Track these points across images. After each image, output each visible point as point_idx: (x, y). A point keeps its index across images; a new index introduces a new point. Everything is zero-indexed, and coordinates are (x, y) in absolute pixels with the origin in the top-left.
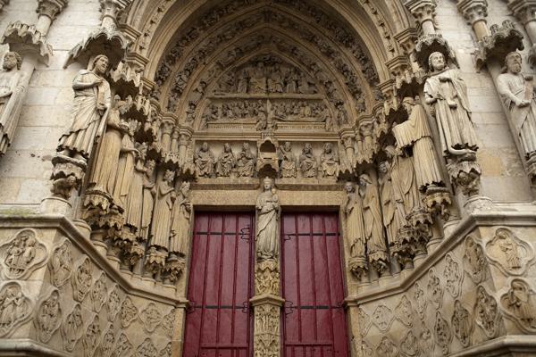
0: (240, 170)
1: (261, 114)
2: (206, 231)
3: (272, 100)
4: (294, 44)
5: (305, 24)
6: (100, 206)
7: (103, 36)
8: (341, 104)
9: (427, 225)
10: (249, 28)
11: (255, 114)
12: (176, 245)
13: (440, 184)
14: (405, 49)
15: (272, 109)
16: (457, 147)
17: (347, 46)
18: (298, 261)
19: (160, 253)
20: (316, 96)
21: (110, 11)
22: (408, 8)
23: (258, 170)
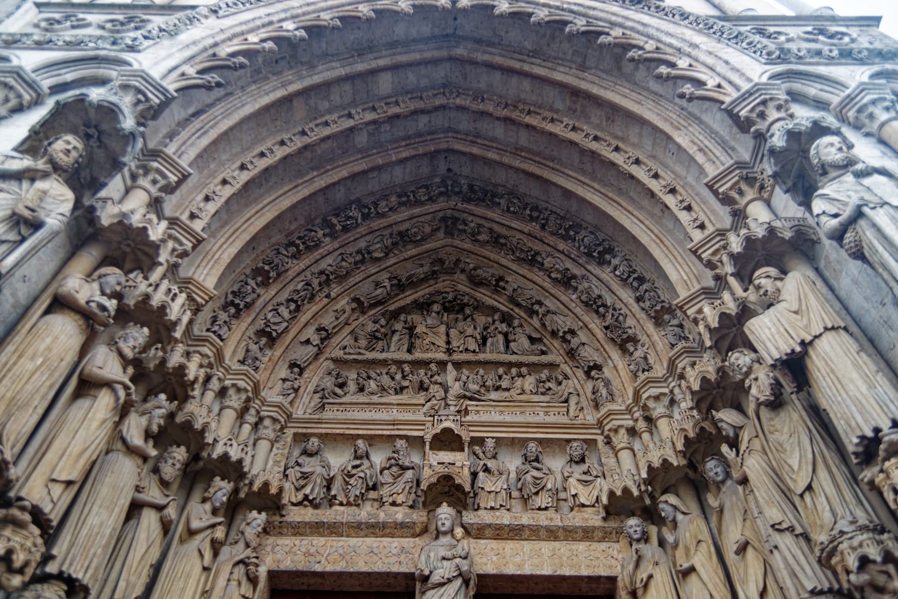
0: (384, 491)
3: (458, 365)
4: (497, 271)
5: (519, 236)
8: (598, 367)
10: (418, 243)
11: (422, 387)
15: (457, 379)
17: (601, 262)
20: (544, 359)
23: (424, 486)
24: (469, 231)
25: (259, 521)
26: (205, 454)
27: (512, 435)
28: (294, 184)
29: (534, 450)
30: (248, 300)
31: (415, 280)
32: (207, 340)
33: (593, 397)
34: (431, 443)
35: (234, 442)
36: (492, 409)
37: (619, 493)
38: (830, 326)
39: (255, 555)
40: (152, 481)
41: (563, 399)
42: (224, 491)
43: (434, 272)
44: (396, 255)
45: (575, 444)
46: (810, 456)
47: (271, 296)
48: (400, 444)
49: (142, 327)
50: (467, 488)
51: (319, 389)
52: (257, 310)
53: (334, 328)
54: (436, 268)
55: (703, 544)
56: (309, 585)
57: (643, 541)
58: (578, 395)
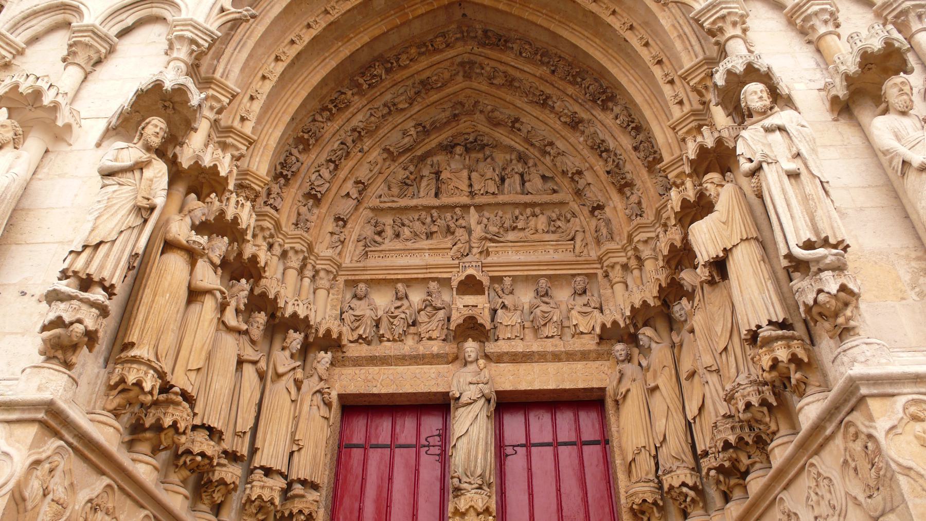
0: (422, 329)
1: (460, 232)
2: (362, 442)
3: (479, 208)
4: (514, 113)
5: (531, 79)
6: (139, 384)
7: (158, 86)
8: (600, 207)
9: (765, 409)
10: (439, 89)
11: (449, 231)
12: (302, 469)
13: (783, 325)
14: (700, 94)
15: (479, 223)
16: (809, 245)
17: (604, 108)
18: (531, 495)
19: (269, 482)
20: (555, 198)
21: (182, 52)
22: (697, 21)
23: (453, 326)
24: (485, 75)
25: (327, 360)
26: (279, 314)
27: (526, 273)
28: (322, 58)
29: (544, 285)
30: (294, 170)
31: (438, 125)
32: (267, 215)
33: (595, 235)
34: (457, 289)
35: (300, 302)
36: (509, 249)
37: (609, 326)
38: (745, 238)
39: (327, 386)
40: (245, 342)
41: (570, 237)
42: (298, 340)
43: (455, 116)
44: (419, 103)
45: (578, 279)
46: (729, 325)
47: (312, 160)
48: (433, 285)
49: (222, 237)
50: (488, 326)
51: (362, 238)
52: (302, 176)
53: (369, 180)
54: (457, 112)
55: (667, 368)
56: (370, 402)
57: (626, 362)
58: (584, 232)
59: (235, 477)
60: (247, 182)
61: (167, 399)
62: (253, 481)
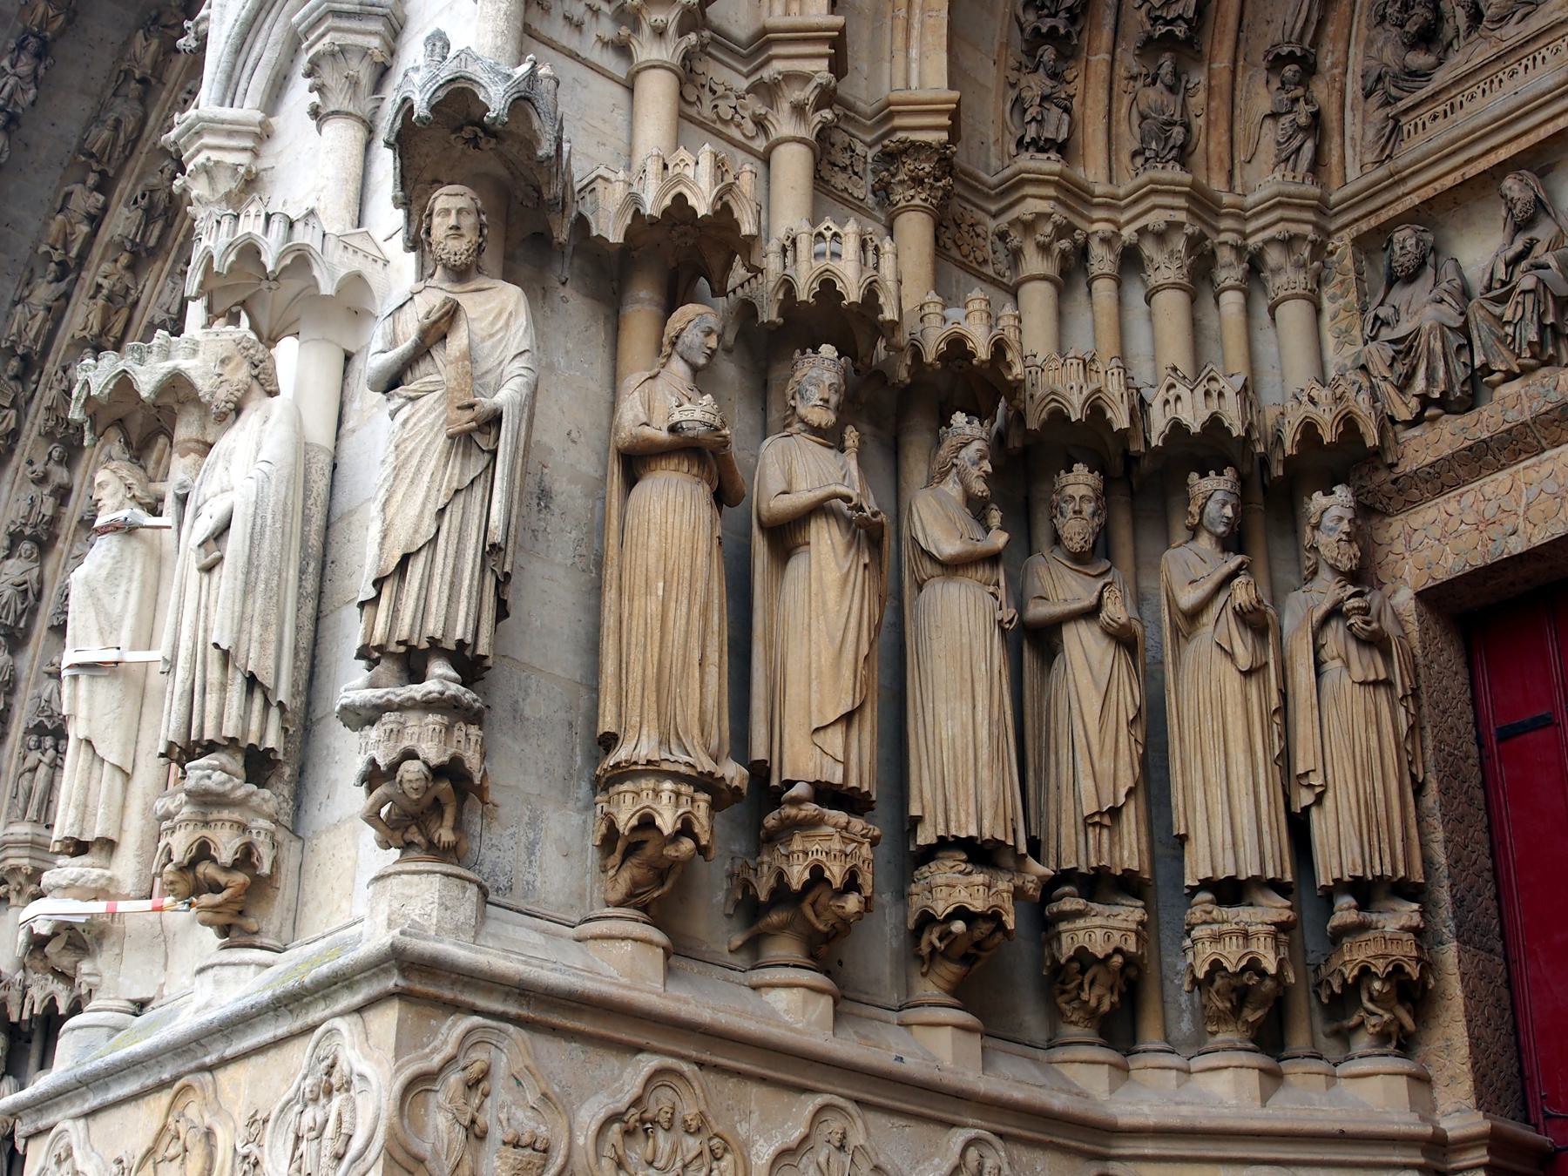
19: (1243, 914)
25: (1335, 512)
32: (1022, 183)
42: (1219, 496)
49: (816, 351)
59: (1117, 936)
60: (901, 135)
61: (781, 819)
62: (1192, 927)
